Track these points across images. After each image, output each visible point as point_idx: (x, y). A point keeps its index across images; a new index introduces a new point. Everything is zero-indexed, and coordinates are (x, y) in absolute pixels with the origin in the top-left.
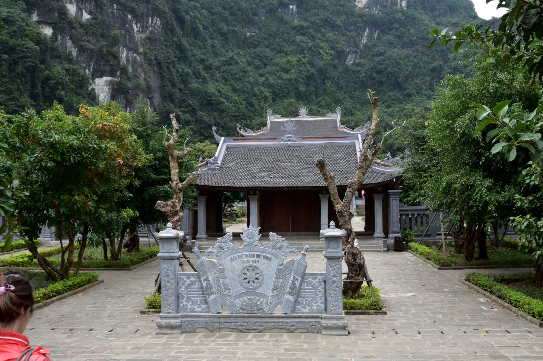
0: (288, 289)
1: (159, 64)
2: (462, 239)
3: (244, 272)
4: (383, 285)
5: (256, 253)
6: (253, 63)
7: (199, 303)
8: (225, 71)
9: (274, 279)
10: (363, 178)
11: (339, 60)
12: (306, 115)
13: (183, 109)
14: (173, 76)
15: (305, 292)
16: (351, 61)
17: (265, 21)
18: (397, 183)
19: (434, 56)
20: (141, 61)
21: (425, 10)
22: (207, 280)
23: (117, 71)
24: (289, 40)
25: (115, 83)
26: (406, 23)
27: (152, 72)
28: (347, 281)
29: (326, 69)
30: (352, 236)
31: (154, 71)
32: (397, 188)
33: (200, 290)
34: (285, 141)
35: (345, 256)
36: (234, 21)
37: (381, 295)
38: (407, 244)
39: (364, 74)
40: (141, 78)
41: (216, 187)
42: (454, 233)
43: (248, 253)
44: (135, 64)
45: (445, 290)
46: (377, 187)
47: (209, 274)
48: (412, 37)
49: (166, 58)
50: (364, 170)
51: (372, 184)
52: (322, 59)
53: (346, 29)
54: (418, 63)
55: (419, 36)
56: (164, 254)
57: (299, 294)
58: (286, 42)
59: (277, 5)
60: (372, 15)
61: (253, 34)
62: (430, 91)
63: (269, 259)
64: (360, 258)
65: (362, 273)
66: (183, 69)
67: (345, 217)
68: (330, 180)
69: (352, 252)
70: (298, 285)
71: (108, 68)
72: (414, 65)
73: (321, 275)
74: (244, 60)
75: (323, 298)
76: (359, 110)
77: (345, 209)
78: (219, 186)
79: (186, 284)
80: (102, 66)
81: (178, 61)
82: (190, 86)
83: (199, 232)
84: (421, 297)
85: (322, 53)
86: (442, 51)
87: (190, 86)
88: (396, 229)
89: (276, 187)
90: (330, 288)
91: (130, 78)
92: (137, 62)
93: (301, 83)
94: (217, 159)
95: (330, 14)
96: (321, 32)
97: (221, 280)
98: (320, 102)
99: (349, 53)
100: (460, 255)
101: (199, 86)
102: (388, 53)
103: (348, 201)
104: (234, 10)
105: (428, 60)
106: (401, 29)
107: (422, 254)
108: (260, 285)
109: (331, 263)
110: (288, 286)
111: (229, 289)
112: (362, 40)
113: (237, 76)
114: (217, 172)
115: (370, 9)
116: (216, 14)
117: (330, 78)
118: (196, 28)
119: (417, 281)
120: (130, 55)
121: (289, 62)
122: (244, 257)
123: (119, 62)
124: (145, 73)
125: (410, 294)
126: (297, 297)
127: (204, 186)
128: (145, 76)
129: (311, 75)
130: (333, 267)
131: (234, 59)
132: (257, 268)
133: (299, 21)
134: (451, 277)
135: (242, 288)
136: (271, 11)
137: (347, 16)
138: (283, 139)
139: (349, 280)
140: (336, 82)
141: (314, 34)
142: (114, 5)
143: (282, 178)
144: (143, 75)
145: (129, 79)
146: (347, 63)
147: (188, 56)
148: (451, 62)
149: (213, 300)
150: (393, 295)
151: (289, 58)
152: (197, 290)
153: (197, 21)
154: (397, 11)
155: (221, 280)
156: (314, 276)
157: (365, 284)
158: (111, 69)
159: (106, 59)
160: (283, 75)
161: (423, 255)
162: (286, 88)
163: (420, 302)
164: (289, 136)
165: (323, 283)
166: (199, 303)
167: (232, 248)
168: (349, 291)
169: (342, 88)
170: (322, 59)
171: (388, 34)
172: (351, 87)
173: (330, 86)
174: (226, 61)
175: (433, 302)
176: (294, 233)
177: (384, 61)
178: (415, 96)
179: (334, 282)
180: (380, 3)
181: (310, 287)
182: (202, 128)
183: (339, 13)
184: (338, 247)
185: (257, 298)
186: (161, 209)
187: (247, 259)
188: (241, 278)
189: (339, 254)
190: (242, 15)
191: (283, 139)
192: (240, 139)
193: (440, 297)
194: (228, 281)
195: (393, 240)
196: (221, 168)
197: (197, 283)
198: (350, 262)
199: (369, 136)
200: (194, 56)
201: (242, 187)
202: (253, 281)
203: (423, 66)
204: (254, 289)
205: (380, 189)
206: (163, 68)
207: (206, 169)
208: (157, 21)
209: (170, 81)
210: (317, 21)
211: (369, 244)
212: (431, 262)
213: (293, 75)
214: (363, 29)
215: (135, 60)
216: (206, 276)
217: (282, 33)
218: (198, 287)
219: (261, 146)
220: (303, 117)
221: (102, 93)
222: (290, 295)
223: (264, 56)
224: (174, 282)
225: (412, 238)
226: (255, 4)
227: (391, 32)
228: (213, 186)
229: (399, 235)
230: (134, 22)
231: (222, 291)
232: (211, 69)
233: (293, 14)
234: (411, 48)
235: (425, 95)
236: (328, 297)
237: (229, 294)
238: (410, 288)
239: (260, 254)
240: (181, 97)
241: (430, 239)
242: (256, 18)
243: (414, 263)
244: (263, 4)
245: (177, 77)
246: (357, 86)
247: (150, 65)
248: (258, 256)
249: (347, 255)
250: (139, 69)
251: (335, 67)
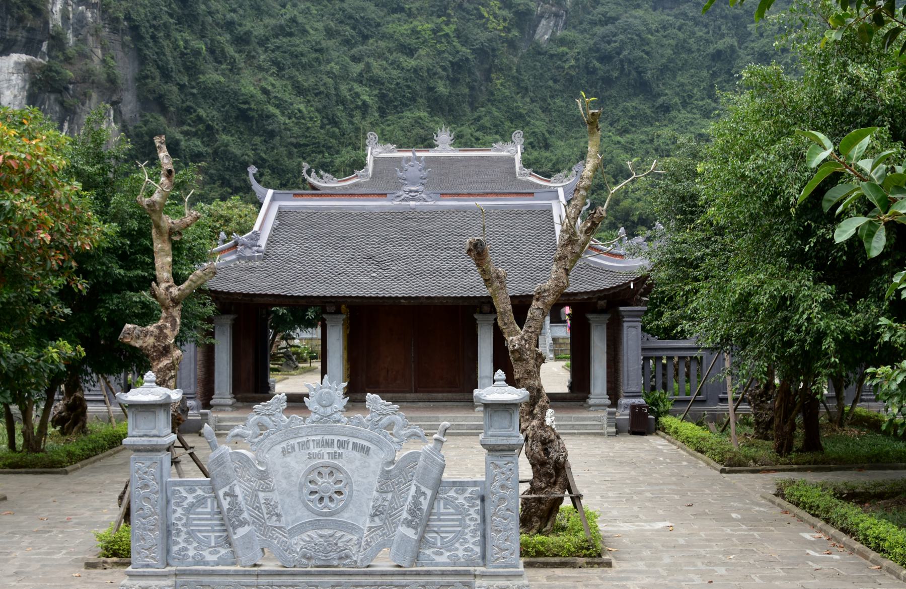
0: (405, 515)
1: (135, 29)
2: (770, 409)
3: (310, 477)
4: (606, 505)
5: (336, 438)
6: (338, 32)
7: (213, 544)
8: (278, 48)
9: (375, 493)
10: (565, 281)
11: (522, 31)
12: (451, 145)
13: (186, 128)
14: (165, 55)
15: (440, 520)
16: (545, 33)
18: (638, 291)
19: (720, 28)
20: (95, 22)
22: (231, 494)
23: (41, 42)
25: (38, 69)
27: (119, 47)
28: (529, 496)
29: (494, 50)
30: (540, 403)
31: (124, 45)
32: (639, 303)
33: (216, 516)
34: (403, 200)
35: (527, 445)
37: (601, 527)
38: (657, 419)
39: (573, 62)
40: (95, 59)
41: (255, 295)
42: (754, 397)
43: (319, 438)
44: (82, 27)
45: (734, 515)
46: (594, 300)
47: (235, 482)
49: (150, 18)
50: (568, 263)
51: (586, 293)
54: (685, 41)
56: (138, 439)
57: (427, 525)
62: (709, 101)
63: (365, 450)
64: (557, 448)
65: (560, 480)
66: (186, 42)
67: (528, 363)
68: (497, 284)
69: (541, 436)
70: (425, 505)
71: (21, 35)
72: (677, 45)
73: (475, 483)
74: (320, 25)
75: (479, 533)
76: (561, 138)
77: (527, 346)
78: (260, 294)
79: (185, 504)
80: (8, 29)
81: (176, 24)
82: (202, 78)
83: (216, 392)
84: (684, 531)
85: (486, 15)
86: (736, 17)
87: (202, 78)
88: (634, 389)
89: (384, 297)
90: (492, 511)
91: (70, 59)
92: (87, 24)
93: (440, 78)
94: (257, 235)
97: (261, 495)
98: (479, 118)
99: (541, 16)
100: (766, 442)
101: (222, 79)
102: (623, 19)
103: (533, 329)
105: (707, 36)
107: (687, 441)
108: (345, 506)
109: (495, 460)
110: (406, 508)
111: (278, 515)
113: (304, 60)
114: (257, 263)
117: (501, 70)
119: (676, 497)
120: (70, 9)
121: (414, 32)
122: (312, 446)
123: (46, 23)
124: (103, 48)
125: (660, 525)
126: (424, 532)
127: (228, 293)
128: (103, 55)
129: (461, 60)
130: (500, 468)
131: (297, 23)
132: (339, 470)
134: (745, 489)
135: (307, 513)
138: (399, 196)
139: (533, 496)
140: (513, 77)
143: (396, 278)
144: (99, 52)
145: (68, 60)
146: (537, 37)
147: (198, 14)
148: (753, 41)
149: (242, 537)
150: (626, 527)
151: (415, 23)
152: (209, 516)
155: (261, 495)
156: (460, 486)
157: (567, 503)
158: (27, 38)
159: (16, 16)
160: (401, 60)
161: (689, 442)
162: (409, 87)
163: (681, 541)
164: (413, 188)
165: (478, 502)
166: (213, 544)
167: (286, 427)
168: (535, 519)
169: (526, 89)
172: (546, 88)
173: (502, 85)
174: (281, 27)
175: (708, 540)
176: (420, 395)
178: (679, 111)
179: (502, 499)
181: (452, 511)
182: (228, 169)
184: (510, 426)
185: (339, 534)
186: (133, 343)
187: (316, 450)
188: (305, 491)
189: (513, 441)
191: (399, 196)
192: (308, 195)
193: (723, 531)
194: (275, 497)
195: (628, 411)
196: (266, 256)
197: (209, 501)
198: (536, 458)
199: (579, 191)
200: (210, 13)
201: (312, 297)
202: (330, 498)
203: (695, 47)
204: (332, 514)
205: (602, 303)
206: (144, 38)
207: (234, 257)
209: (158, 67)
211: (577, 419)
212: (705, 457)
213: (423, 59)
215: (81, 21)
216: (228, 487)
218: (212, 509)
219: (352, 209)
220: (444, 150)
221: (8, 88)
222: (408, 526)
223: (362, 18)
224: (160, 499)
225: (666, 408)
228: (248, 295)
229: (641, 401)
231: (263, 518)
232: (248, 43)
234: (671, 9)
235: (699, 108)
236: (488, 530)
237: (278, 524)
238: (661, 512)
239: (345, 439)
240: (183, 102)
241: (705, 409)
243: (671, 459)
245: (174, 58)
246: (557, 87)
247: (115, 30)
248: (342, 444)
249: (529, 442)
250: (90, 39)
251: (512, 45)
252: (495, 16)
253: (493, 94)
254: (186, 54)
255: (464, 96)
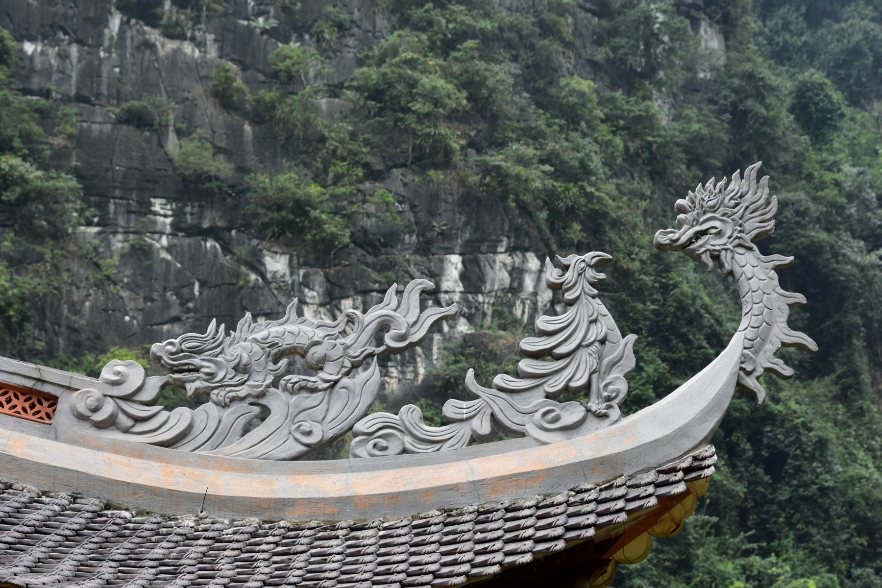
142: (157, 205)
147: (823, 490)
208: (517, 273)
230: (311, 295)
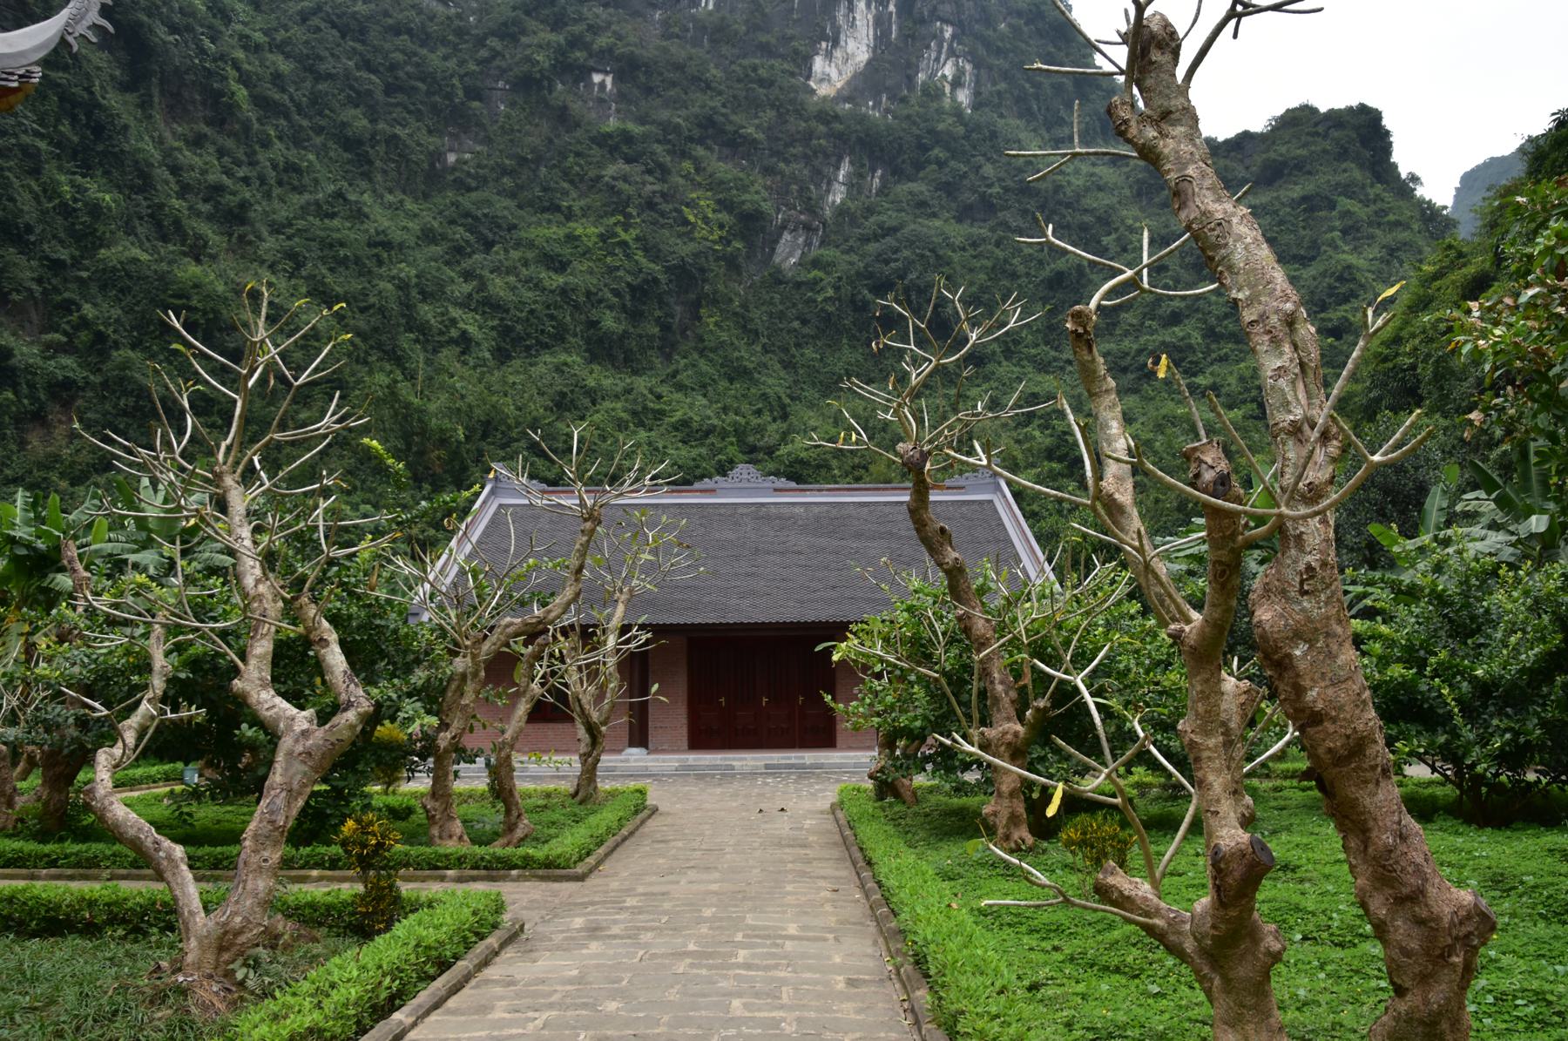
6: (444, 237)
11: (750, 245)
16: (791, 254)
17: (508, 117)
21: (1028, 122)
24: (582, 180)
26: (968, 148)
29: (702, 270)
36: (399, 109)
39: (830, 292)
48: (990, 186)
52: (688, 236)
53: (775, 153)
54: (1006, 261)
55: (1009, 183)
58: (572, 182)
59: (547, 65)
60: (863, 119)
61: (467, 156)
72: (994, 268)
76: (811, 406)
85: (692, 218)
93: (611, 308)
95: (724, 106)
96: (690, 157)
98: (675, 374)
99: (783, 227)
104: (401, 74)
105: (1041, 256)
106: (952, 163)
112: (828, 191)
115: (856, 105)
116: (329, 76)
117: (715, 302)
118: (221, 94)
121: (571, 238)
129: (646, 281)
131: (345, 200)
133: (623, 120)
136: (529, 85)
137: (780, 115)
140: (735, 314)
141: (668, 158)
146: (777, 259)
147: (122, 151)
153: (232, 73)
154: (941, 111)
160: (543, 275)
162: (552, 317)
169: (756, 333)
170: (688, 236)
171: (910, 180)
172: (789, 332)
173: (716, 324)
177: (896, 251)
180: (887, 89)
182: (125, 413)
183: (755, 105)
190: (429, 93)
203: (1021, 269)
210: (680, 120)
213: (581, 276)
214: (833, 159)
217: (560, 153)
223: (486, 215)
226: (479, 63)
227: (921, 174)
232: (243, 221)
233: (601, 101)
235: (1032, 359)
242: (476, 104)
244: (504, 64)
246: (806, 330)
251: (732, 264)
252: (706, 220)
253: (701, 340)
254: (75, 210)
255: (651, 338)
